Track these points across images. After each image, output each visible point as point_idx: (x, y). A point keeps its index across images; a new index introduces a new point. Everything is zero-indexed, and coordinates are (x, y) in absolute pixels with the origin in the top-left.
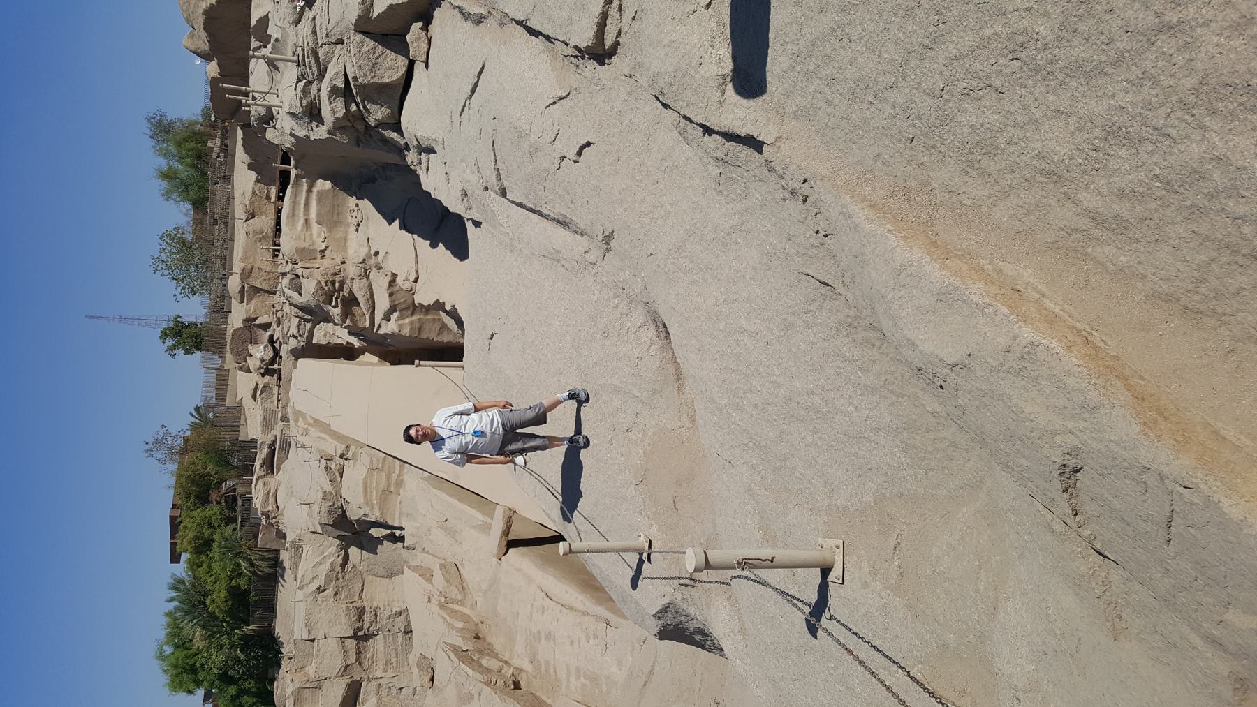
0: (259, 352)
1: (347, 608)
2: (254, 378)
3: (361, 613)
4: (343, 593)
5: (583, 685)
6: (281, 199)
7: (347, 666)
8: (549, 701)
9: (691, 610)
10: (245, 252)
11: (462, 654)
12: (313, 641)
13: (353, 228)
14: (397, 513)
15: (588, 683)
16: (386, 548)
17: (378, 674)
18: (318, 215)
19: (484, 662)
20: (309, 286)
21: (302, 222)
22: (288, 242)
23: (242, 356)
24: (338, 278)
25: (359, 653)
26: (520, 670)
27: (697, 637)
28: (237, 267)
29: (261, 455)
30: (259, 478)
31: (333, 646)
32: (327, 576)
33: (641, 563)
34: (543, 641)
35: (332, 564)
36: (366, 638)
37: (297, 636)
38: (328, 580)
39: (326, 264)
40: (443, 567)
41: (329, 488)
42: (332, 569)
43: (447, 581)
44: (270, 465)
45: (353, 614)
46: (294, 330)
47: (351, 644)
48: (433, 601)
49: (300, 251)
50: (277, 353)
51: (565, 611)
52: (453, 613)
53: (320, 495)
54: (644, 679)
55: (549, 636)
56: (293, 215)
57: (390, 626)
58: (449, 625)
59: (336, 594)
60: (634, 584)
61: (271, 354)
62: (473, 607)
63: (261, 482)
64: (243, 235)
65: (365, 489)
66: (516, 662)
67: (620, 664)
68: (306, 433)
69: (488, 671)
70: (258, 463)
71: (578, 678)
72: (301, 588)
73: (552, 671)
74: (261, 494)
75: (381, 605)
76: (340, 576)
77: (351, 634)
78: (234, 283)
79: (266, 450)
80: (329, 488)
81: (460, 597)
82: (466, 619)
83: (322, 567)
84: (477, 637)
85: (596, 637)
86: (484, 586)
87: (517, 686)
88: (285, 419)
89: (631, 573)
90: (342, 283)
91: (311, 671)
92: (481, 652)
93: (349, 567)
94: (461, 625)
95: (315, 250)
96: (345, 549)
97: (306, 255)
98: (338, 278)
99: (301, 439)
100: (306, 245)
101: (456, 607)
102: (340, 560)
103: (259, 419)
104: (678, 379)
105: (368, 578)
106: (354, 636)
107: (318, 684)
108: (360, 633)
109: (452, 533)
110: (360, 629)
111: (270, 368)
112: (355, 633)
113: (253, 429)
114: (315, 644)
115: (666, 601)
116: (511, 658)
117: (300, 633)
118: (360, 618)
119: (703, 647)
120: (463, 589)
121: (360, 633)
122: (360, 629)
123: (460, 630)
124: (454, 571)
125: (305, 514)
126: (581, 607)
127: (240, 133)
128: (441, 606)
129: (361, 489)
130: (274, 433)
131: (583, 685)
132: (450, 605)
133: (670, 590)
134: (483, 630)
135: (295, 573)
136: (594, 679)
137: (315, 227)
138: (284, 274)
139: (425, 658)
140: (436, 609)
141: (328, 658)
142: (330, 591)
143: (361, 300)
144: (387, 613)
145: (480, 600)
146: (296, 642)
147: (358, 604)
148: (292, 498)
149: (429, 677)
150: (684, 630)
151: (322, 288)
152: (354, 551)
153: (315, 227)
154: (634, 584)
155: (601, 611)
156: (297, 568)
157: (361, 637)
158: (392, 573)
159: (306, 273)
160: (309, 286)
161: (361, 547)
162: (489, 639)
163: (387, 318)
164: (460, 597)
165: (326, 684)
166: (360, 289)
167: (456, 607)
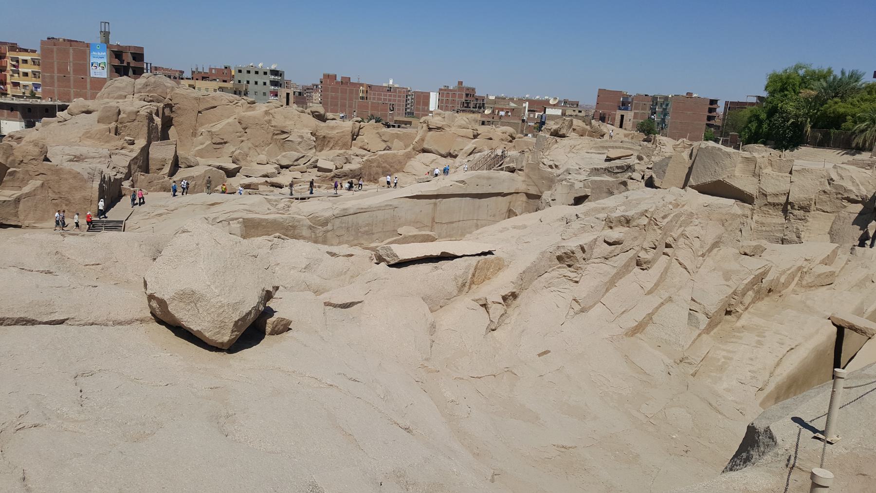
1: (811, 199)
3: (805, 209)
4: (824, 197)
5: (719, 360)
7: (766, 196)
8: (712, 333)
9: (768, 457)
11: (760, 278)
12: (791, 173)
15: (720, 364)
16: (857, 232)
17: (755, 217)
19: (751, 293)
25: (774, 205)
26: (739, 317)
27: (744, 455)
31: (784, 187)
33: (814, 430)
34: (757, 338)
35: (851, 191)
36: (785, 211)
37: (796, 162)
38: (837, 187)
40: (832, 274)
42: (846, 190)
43: (819, 276)
45: (806, 203)
47: (783, 199)
48: (806, 263)
51: (777, 360)
52: (792, 276)
54: (714, 404)
55: (760, 343)
57: (791, 229)
58: (784, 272)
59: (825, 192)
60: (796, 420)
62: (794, 291)
66: (746, 316)
67: (728, 390)
69: (744, 294)
71: (724, 357)
72: (835, 167)
73: (733, 340)
75: (808, 224)
76: (839, 196)
77: (790, 200)
81: (804, 283)
82: (786, 285)
83: (850, 183)
84: (770, 291)
85: (752, 378)
86: (808, 302)
87: (728, 313)
89: (806, 420)
91: (768, 170)
92: (758, 292)
93: (845, 203)
94: (782, 280)
96: (863, 202)
101: (796, 279)
102: (853, 197)
105: (832, 217)
106: (787, 202)
107: (757, 175)
108: (789, 207)
109: (860, 284)
110: (793, 208)
112: (790, 203)
114: (788, 174)
115: (779, 441)
116: (749, 313)
117: (798, 164)
118: (801, 208)
119: (735, 456)
120: (810, 286)
121: (789, 207)
122: (793, 208)
123: (778, 279)
124: (827, 281)
126: (779, 370)
128: (800, 268)
131: (719, 360)
132: (799, 274)
133: (787, 446)
134: (774, 296)
135: (849, 163)
136: (721, 369)
139: (762, 251)
140: (799, 264)
141: (775, 182)
142: (828, 188)
145: (798, 298)
147: (813, 207)
149: (748, 252)
150: (752, 447)
152: (859, 207)
154: (796, 420)
155: (771, 387)
156: (853, 164)
157: (786, 208)
158: (833, 235)
161: (861, 214)
162: (767, 299)
164: (804, 283)
165: (756, 180)
167: (796, 279)
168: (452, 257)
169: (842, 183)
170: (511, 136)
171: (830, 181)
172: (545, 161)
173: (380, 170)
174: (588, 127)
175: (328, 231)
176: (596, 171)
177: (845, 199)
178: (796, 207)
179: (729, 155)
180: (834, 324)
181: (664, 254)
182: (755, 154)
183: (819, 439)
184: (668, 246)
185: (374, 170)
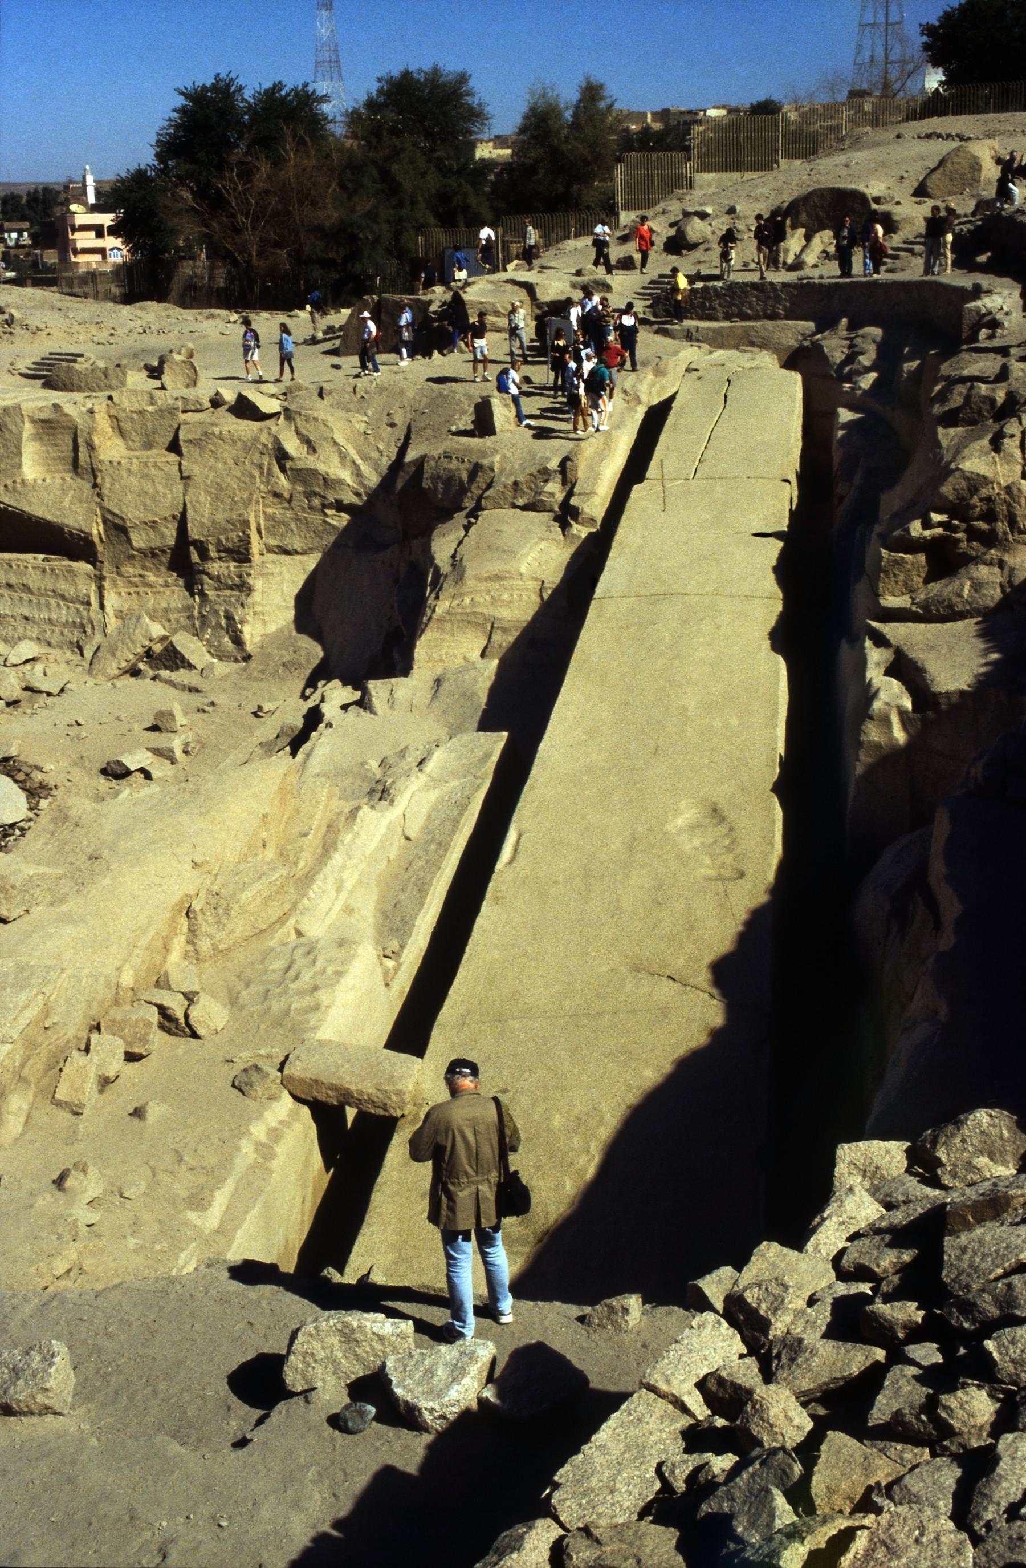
17: (112, 600)
24: (1002, 526)
25: (152, 553)
32: (314, 472)
35: (340, 482)
38: (302, 475)
42: (327, 482)
76: (317, 502)
77: (194, 532)
83: (335, 460)
90: (990, 540)
98: (1002, 526)
108: (195, 558)
112: (196, 543)
122: (204, 555)
142: (283, 482)
147: (256, 546)
151: (973, 489)
169: (311, 462)
177: (330, 506)
178: (213, 554)
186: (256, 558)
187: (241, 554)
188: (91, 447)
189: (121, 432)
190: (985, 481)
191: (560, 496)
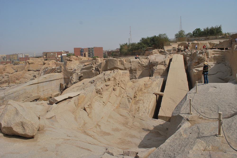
0: (182, 48)
2: (177, 47)
6: (219, 49)
10: (202, 43)
13: (214, 62)
14: (156, 75)
18: (216, 56)
20: (201, 55)
21: (214, 53)
22: (209, 51)
23: (181, 45)
28: (199, 42)
29: (163, 50)
30: (158, 50)
31: (130, 66)
34: (142, 102)
39: (206, 58)
41: (159, 62)
42: (143, 65)
44: (161, 52)
46: (189, 53)
49: (208, 53)
50: (182, 51)
53: (158, 61)
54: (141, 119)
56: (215, 51)
61: (182, 50)
63: (157, 51)
64: (206, 42)
65: (160, 69)
68: (168, 57)
70: (161, 50)
73: (138, 103)
74: (155, 51)
77: (132, 69)
78: (196, 42)
79: (164, 51)
80: (159, 62)
83: (144, 63)
88: (170, 54)
95: (208, 56)
97: (207, 54)
99: (167, 57)
100: (209, 54)
102: (145, 66)
103: (169, 49)
104: (225, 118)
111: (179, 51)
113: (166, 48)
125: (153, 59)
126: (149, 108)
127: (228, 40)
129: (160, 68)
130: (167, 52)
137: (214, 55)
138: (202, 50)
141: (128, 65)
143: (199, 65)
144: (136, 75)
146: (130, 60)
148: (156, 56)
153: (214, 55)
159: (204, 55)
160: (201, 55)
163: (196, 70)
166: (202, 65)
168: (71, 98)
170: (55, 63)
171: (139, 63)
172: (68, 68)
173: (15, 79)
174: (77, 58)
175: (4, 101)
176: (82, 69)
179: (115, 60)
180: (155, 95)
181: (118, 86)
182: (122, 59)
183: (190, 114)
184: (118, 84)
185: (13, 79)
186: (137, 71)
187: (136, 70)
188: (124, 62)
189: (126, 61)
190: (202, 57)
191: (164, 64)
